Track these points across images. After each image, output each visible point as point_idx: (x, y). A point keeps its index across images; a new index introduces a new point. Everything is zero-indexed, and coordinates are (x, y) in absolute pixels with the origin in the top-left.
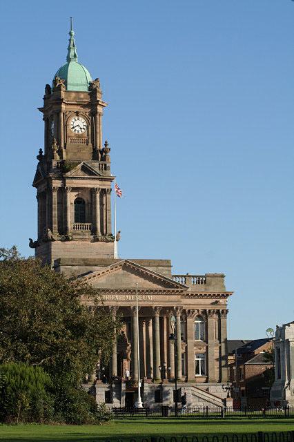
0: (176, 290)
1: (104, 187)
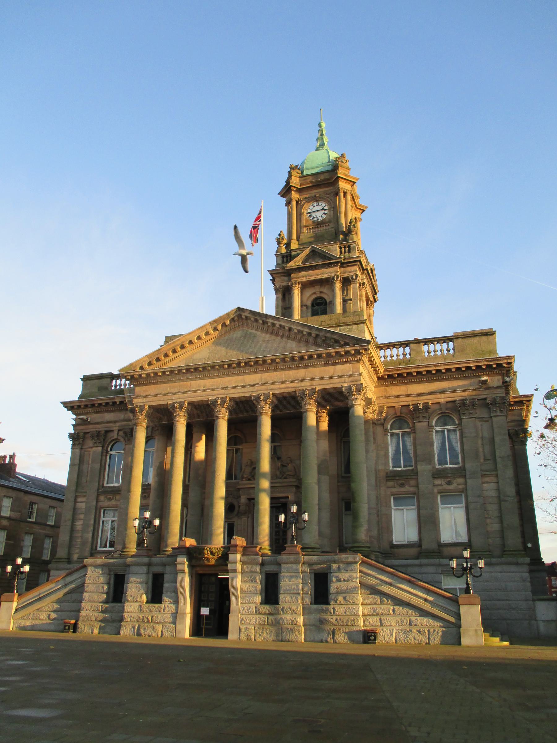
0: (342, 350)
1: (346, 275)
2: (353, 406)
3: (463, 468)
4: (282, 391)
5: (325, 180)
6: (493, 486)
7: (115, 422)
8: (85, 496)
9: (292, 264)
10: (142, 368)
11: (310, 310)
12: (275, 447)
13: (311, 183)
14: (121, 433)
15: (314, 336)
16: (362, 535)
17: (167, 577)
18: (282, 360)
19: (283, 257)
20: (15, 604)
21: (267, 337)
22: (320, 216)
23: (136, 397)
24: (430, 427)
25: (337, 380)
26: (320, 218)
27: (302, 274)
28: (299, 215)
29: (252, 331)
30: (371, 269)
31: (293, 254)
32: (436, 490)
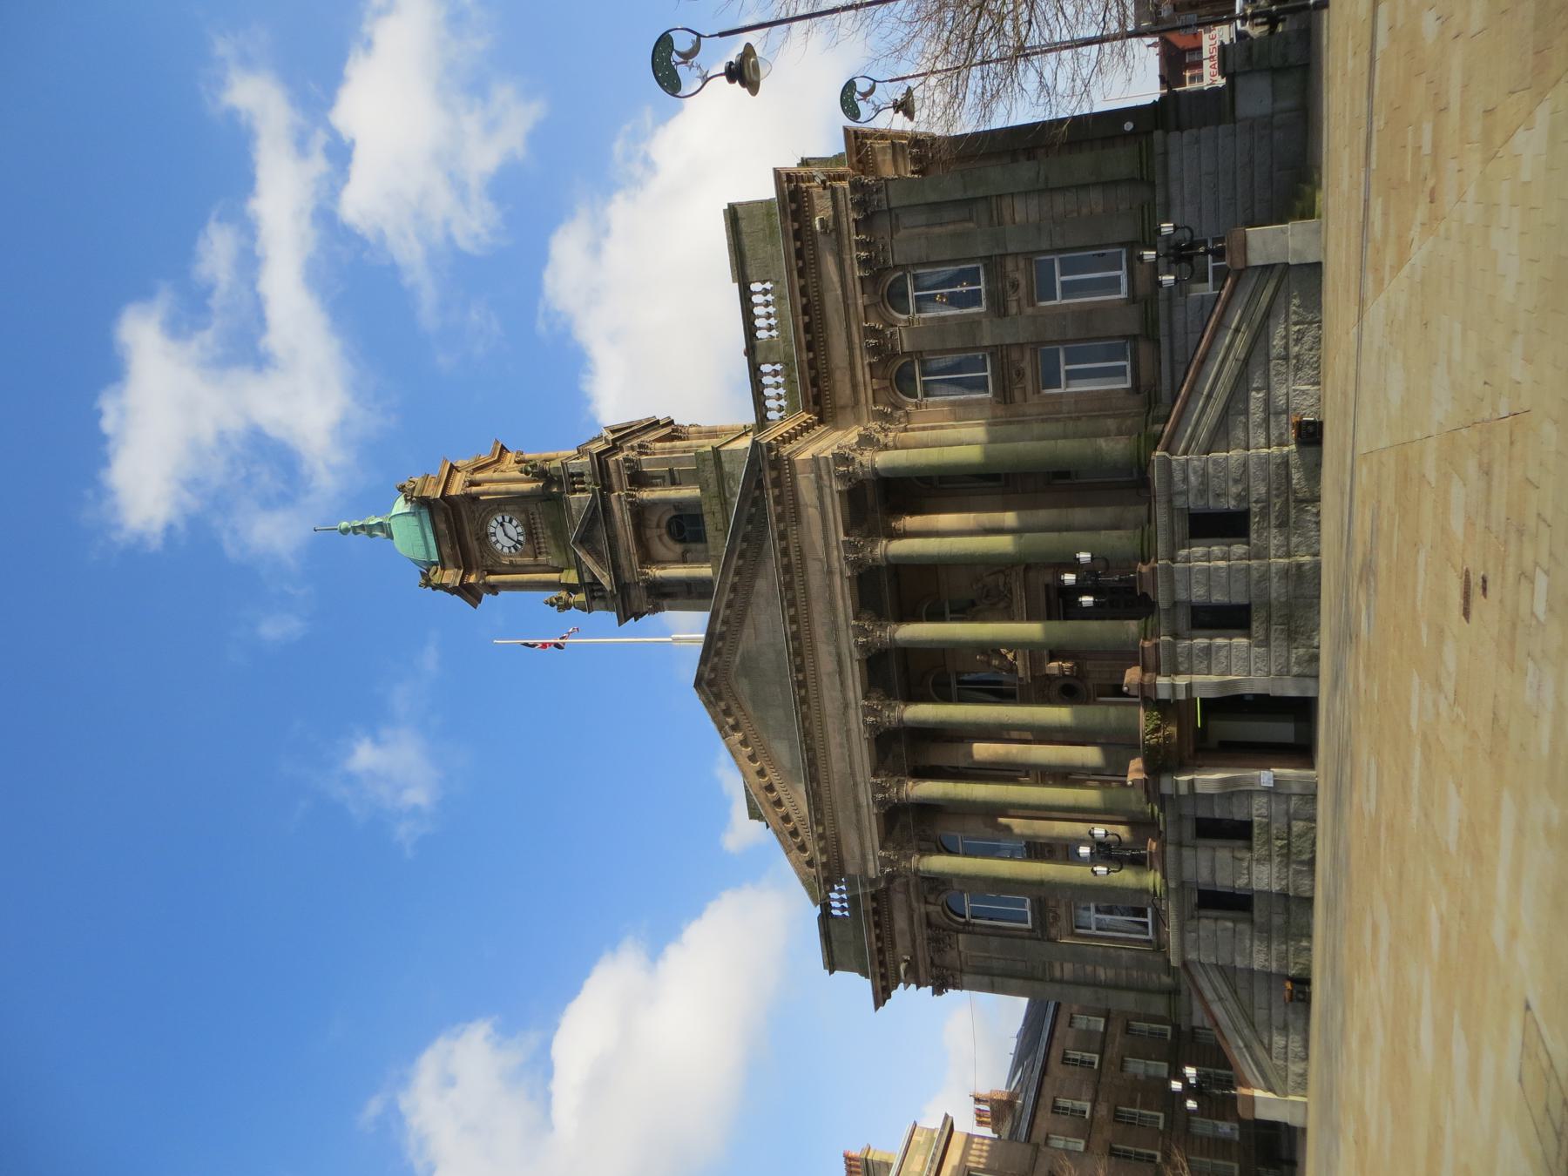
0: (771, 494)
1: (625, 479)
2: (875, 471)
4: (849, 602)
5: (447, 521)
6: (1019, 205)
7: (911, 909)
8: (1051, 965)
9: (606, 580)
10: (810, 863)
11: (693, 546)
12: (952, 612)
13: (453, 548)
14: (931, 898)
15: (745, 545)
16: (1114, 447)
17: (1203, 813)
18: (792, 604)
19: (594, 598)
20: (1258, 1093)
21: (748, 631)
22: (515, 530)
23: (866, 871)
25: (828, 500)
26: (520, 530)
27: (624, 562)
28: (515, 568)
30: (613, 432)
31: (587, 579)
32: (1029, 311)
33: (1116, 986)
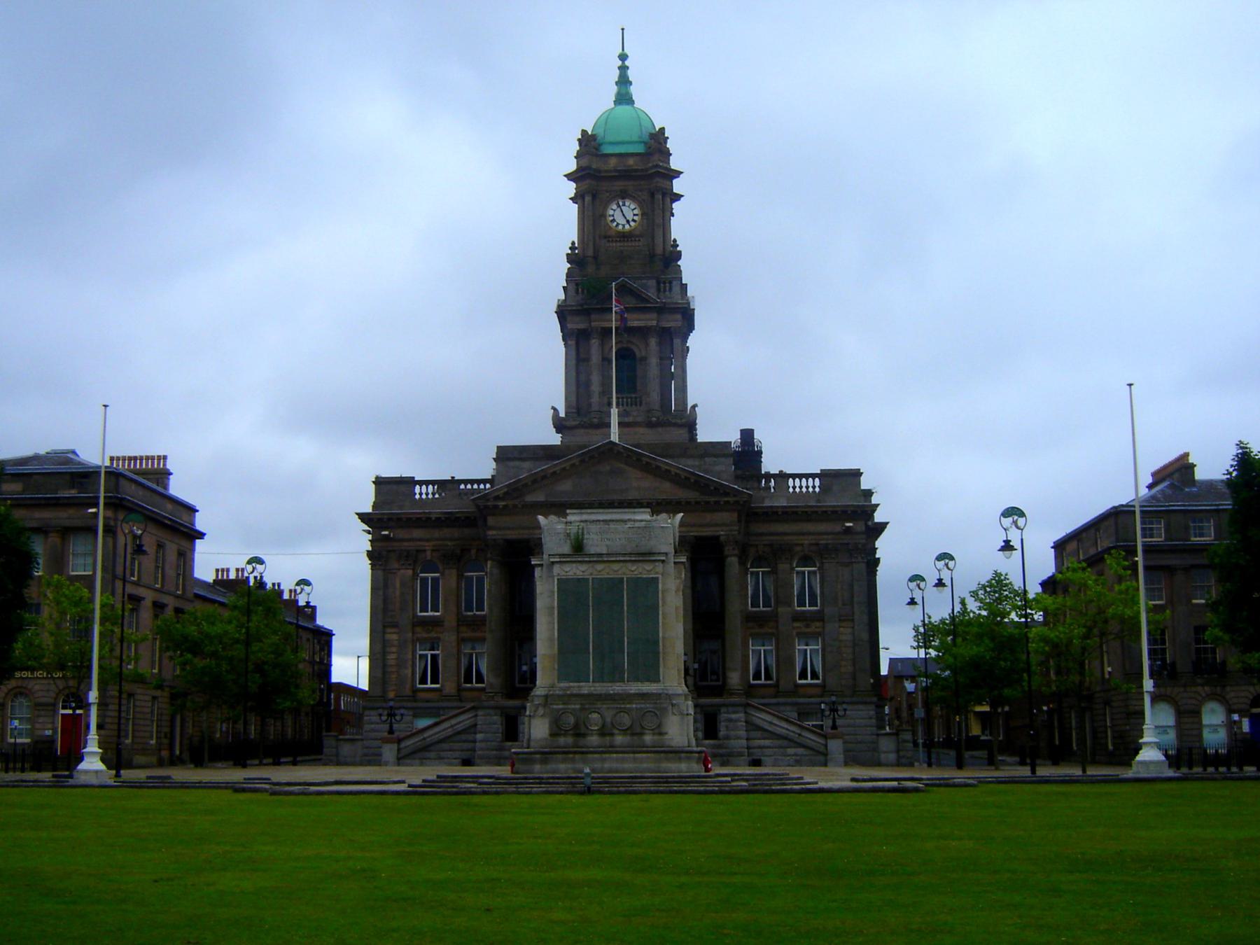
3: (821, 612)
7: (428, 540)
19: (577, 285)
24: (793, 569)
29: (622, 466)
33: (384, 666)
